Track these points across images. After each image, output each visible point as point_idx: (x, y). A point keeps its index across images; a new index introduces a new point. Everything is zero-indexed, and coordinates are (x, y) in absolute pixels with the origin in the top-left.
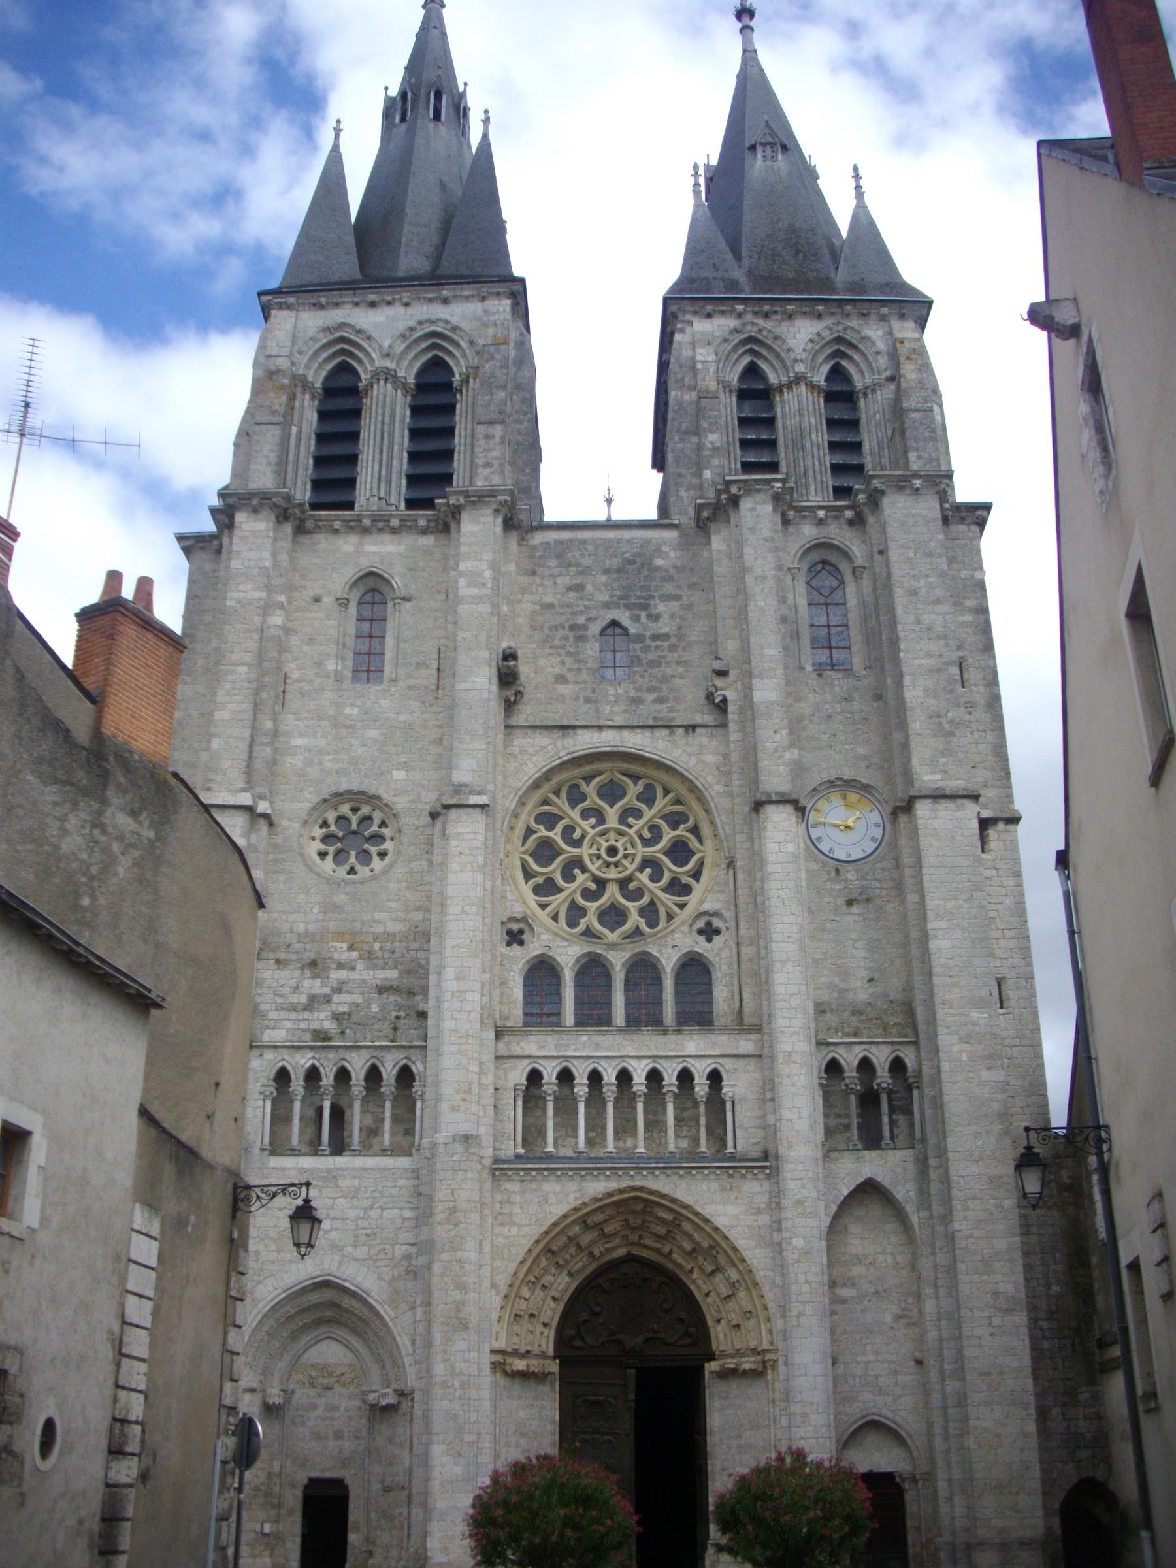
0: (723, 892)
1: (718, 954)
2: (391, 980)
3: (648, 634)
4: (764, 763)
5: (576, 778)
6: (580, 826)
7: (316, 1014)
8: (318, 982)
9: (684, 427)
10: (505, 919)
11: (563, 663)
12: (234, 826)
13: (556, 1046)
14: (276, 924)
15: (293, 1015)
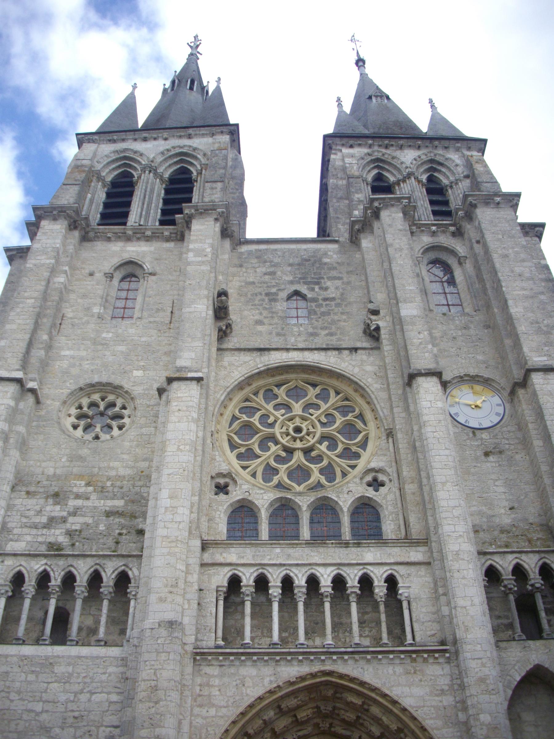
0: (386, 455)
1: (385, 498)
2: (118, 507)
3: (320, 298)
4: (412, 351)
5: (270, 384)
6: (273, 415)
7: (53, 531)
8: (58, 508)
9: (339, 196)
10: (214, 475)
11: (261, 314)
12: (7, 392)
13: (253, 556)
14: (31, 469)
15: (34, 531)
